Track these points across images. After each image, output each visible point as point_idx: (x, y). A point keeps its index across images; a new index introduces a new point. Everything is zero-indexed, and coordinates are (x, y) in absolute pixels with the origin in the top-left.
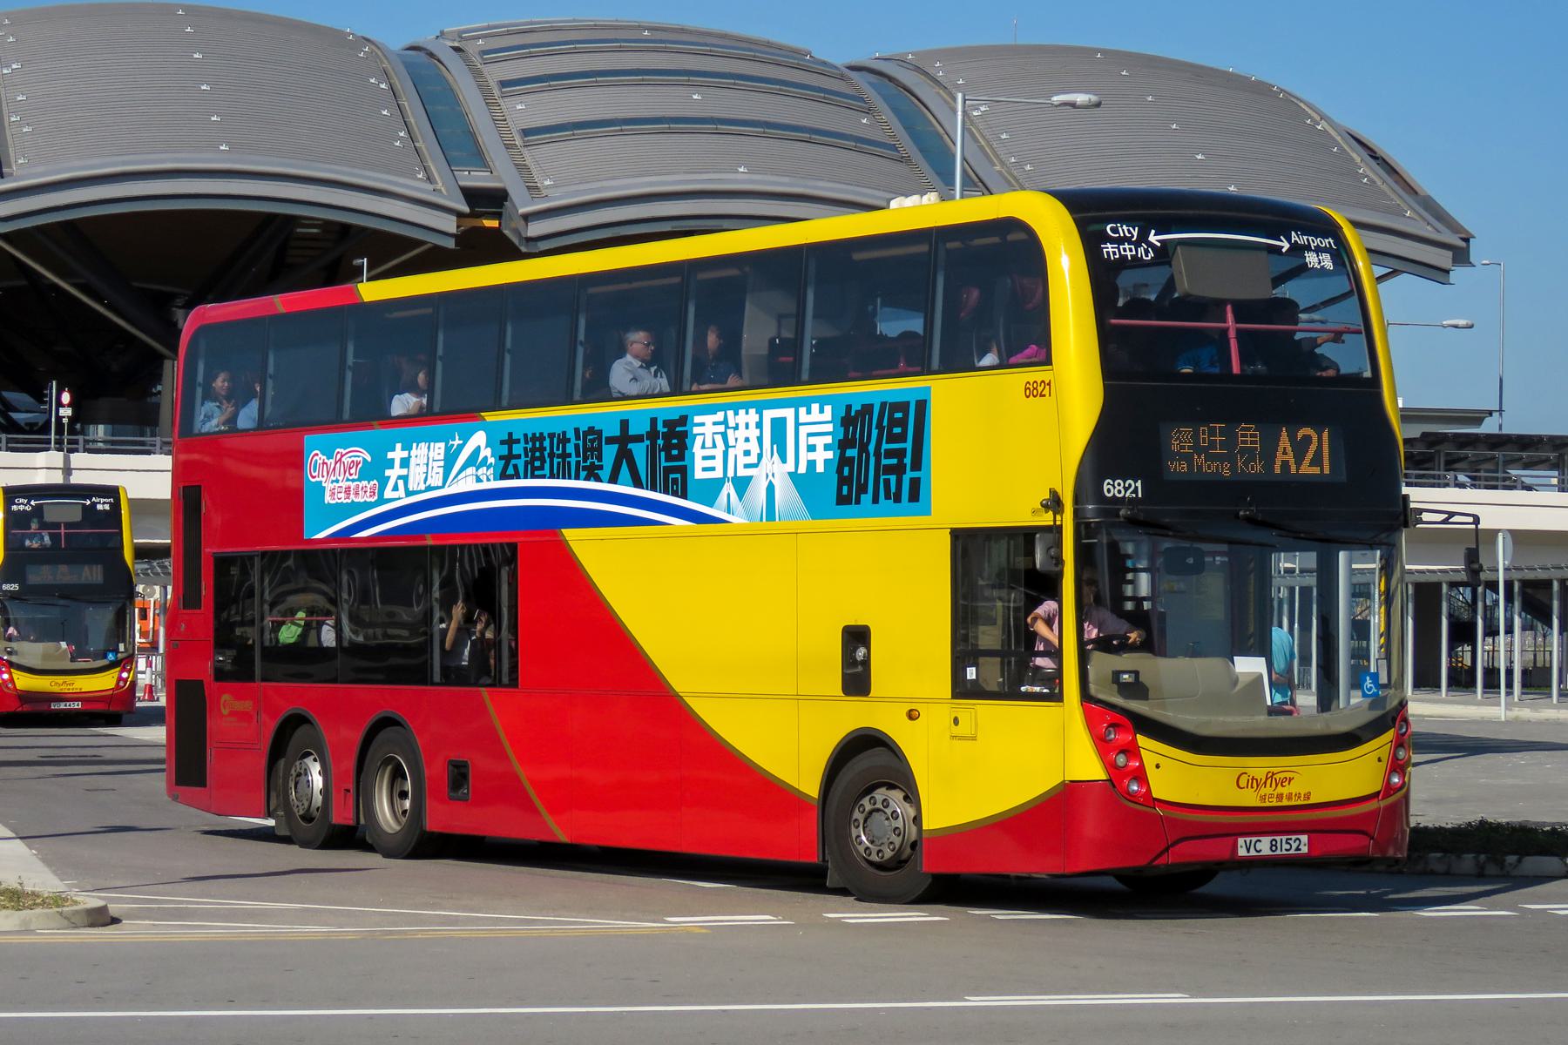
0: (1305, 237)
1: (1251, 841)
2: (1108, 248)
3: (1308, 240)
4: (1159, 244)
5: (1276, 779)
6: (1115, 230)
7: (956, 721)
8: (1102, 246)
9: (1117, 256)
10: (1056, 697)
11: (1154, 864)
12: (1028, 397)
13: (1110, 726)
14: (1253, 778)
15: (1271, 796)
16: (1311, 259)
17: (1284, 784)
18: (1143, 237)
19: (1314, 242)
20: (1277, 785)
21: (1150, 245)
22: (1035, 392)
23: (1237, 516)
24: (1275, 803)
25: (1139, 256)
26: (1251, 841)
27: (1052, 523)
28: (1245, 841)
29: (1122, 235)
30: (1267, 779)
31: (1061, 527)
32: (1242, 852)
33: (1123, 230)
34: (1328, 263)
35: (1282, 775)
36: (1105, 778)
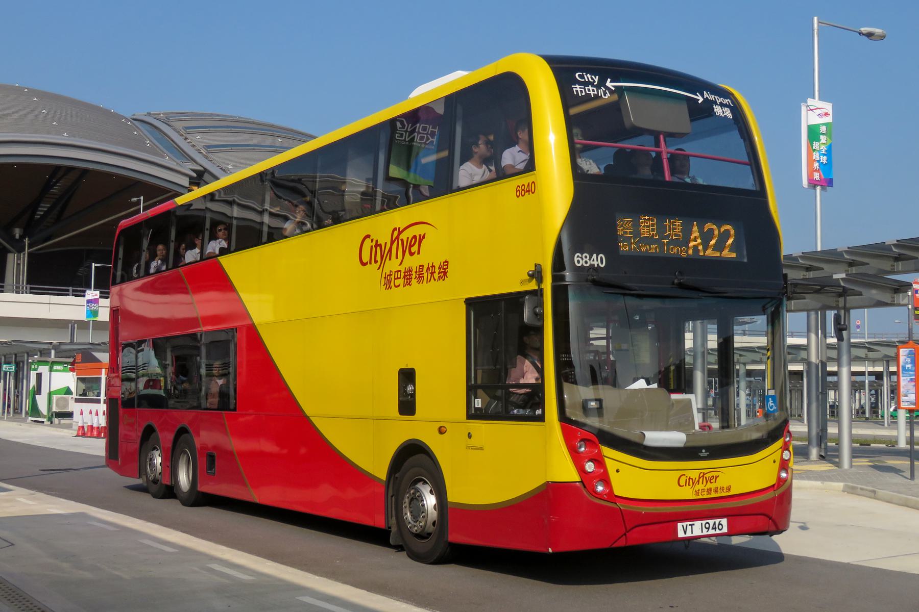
0: (713, 96)
1: (687, 525)
2: (576, 88)
3: (714, 98)
4: (613, 89)
5: (706, 478)
6: (582, 77)
7: (470, 436)
8: (573, 86)
9: (584, 94)
10: (541, 418)
11: (614, 546)
12: (518, 197)
13: (582, 440)
14: (690, 479)
15: (703, 490)
16: (718, 110)
17: (712, 481)
18: (602, 83)
19: (718, 100)
20: (707, 482)
21: (607, 88)
22: (523, 194)
23: (673, 282)
24: (706, 496)
25: (600, 95)
26: (687, 525)
27: (536, 288)
28: (683, 526)
29: (587, 80)
30: (700, 478)
31: (542, 290)
32: (681, 534)
33: (588, 78)
34: (728, 113)
35: (710, 475)
36: (578, 480)
